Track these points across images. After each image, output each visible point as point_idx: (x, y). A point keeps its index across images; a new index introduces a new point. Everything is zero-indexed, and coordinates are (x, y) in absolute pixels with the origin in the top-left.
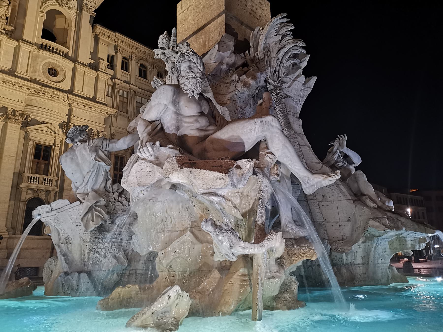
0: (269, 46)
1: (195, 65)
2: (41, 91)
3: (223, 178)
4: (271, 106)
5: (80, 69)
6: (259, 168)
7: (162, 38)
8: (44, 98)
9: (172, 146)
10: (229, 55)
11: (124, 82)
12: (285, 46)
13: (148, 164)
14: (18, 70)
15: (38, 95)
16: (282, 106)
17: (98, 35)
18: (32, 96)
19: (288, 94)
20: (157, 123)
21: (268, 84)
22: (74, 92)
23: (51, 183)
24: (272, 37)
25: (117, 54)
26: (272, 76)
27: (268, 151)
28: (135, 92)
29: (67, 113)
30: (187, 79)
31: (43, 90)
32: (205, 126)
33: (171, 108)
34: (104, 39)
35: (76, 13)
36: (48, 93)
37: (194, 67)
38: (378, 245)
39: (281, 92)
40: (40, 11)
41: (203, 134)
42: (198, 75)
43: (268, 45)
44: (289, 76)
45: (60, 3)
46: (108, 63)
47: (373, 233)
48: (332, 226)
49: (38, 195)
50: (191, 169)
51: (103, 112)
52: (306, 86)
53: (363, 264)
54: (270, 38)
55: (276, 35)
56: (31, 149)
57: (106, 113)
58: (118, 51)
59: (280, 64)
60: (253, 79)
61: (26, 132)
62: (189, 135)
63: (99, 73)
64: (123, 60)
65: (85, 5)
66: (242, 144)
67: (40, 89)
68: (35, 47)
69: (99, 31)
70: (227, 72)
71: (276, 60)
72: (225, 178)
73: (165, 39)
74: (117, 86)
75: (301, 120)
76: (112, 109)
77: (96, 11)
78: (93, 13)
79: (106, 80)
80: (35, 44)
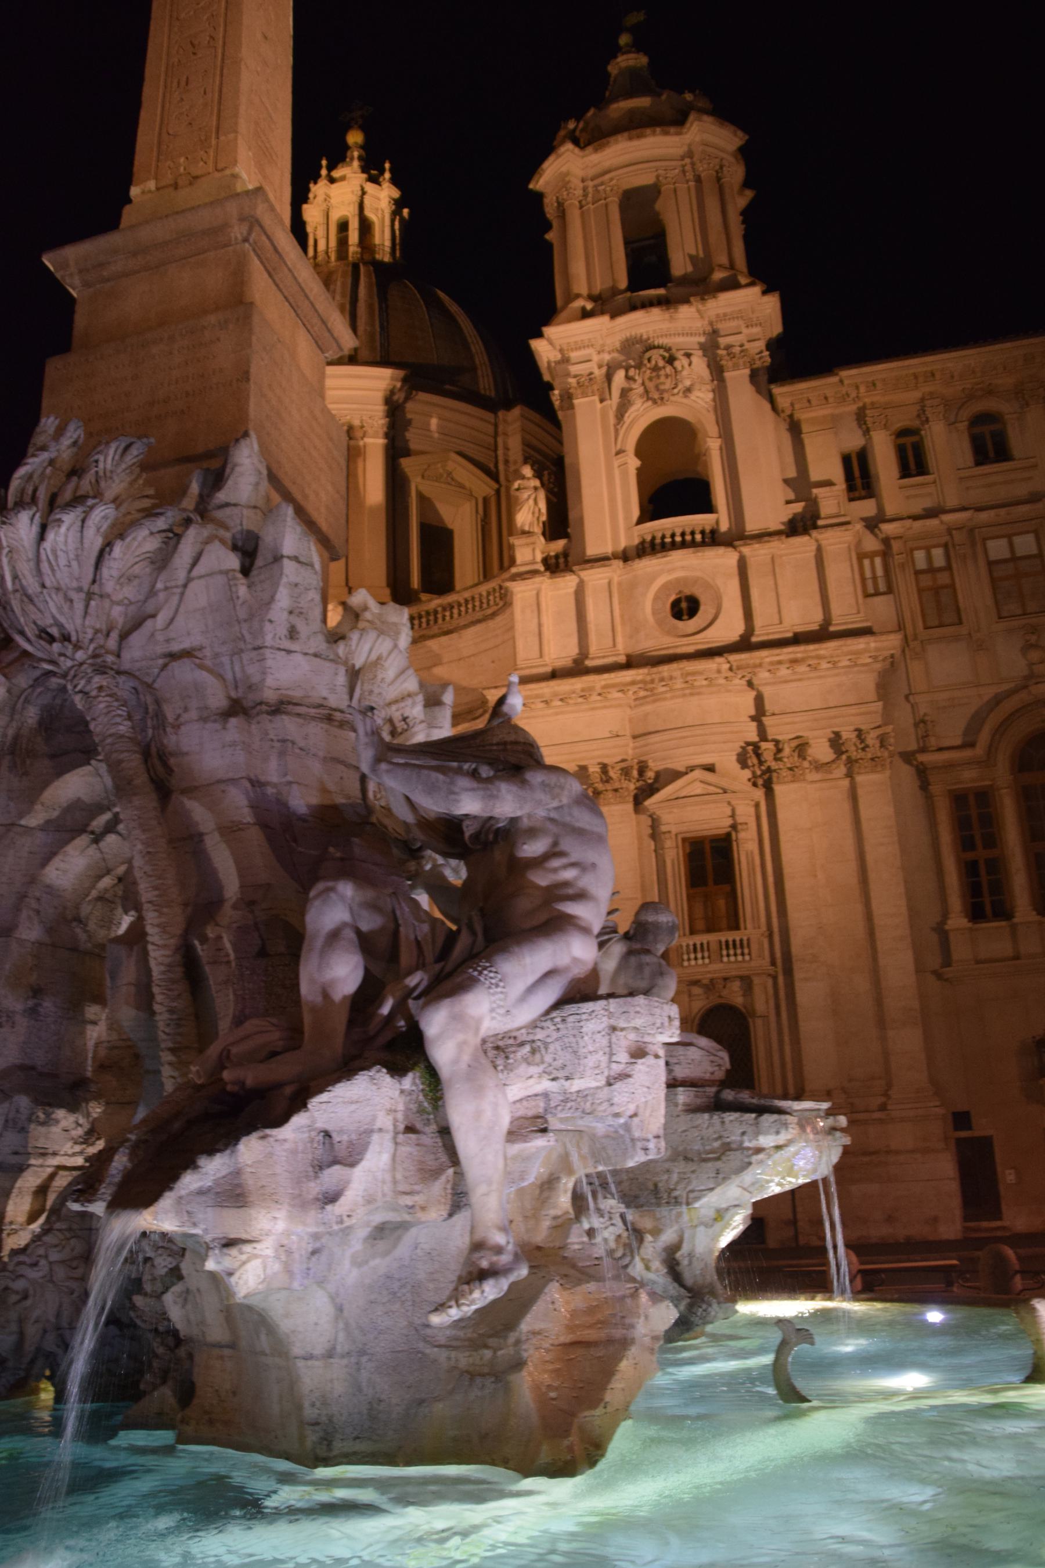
2: (652, 681)
8: (672, 698)
14: (593, 649)
15: (653, 695)
18: (641, 705)
19: (176, 647)
23: (746, 951)
25: (870, 438)
29: (753, 712)
31: (656, 677)
35: (713, 391)
36: (671, 678)
40: (618, 453)
45: (656, 396)
49: (720, 997)
51: (860, 662)
52: (259, 562)
56: (673, 861)
57: (870, 660)
61: (651, 816)
63: (820, 537)
67: (648, 678)
68: (618, 564)
69: (789, 400)
74: (896, 546)
78: (760, 358)
80: (615, 556)
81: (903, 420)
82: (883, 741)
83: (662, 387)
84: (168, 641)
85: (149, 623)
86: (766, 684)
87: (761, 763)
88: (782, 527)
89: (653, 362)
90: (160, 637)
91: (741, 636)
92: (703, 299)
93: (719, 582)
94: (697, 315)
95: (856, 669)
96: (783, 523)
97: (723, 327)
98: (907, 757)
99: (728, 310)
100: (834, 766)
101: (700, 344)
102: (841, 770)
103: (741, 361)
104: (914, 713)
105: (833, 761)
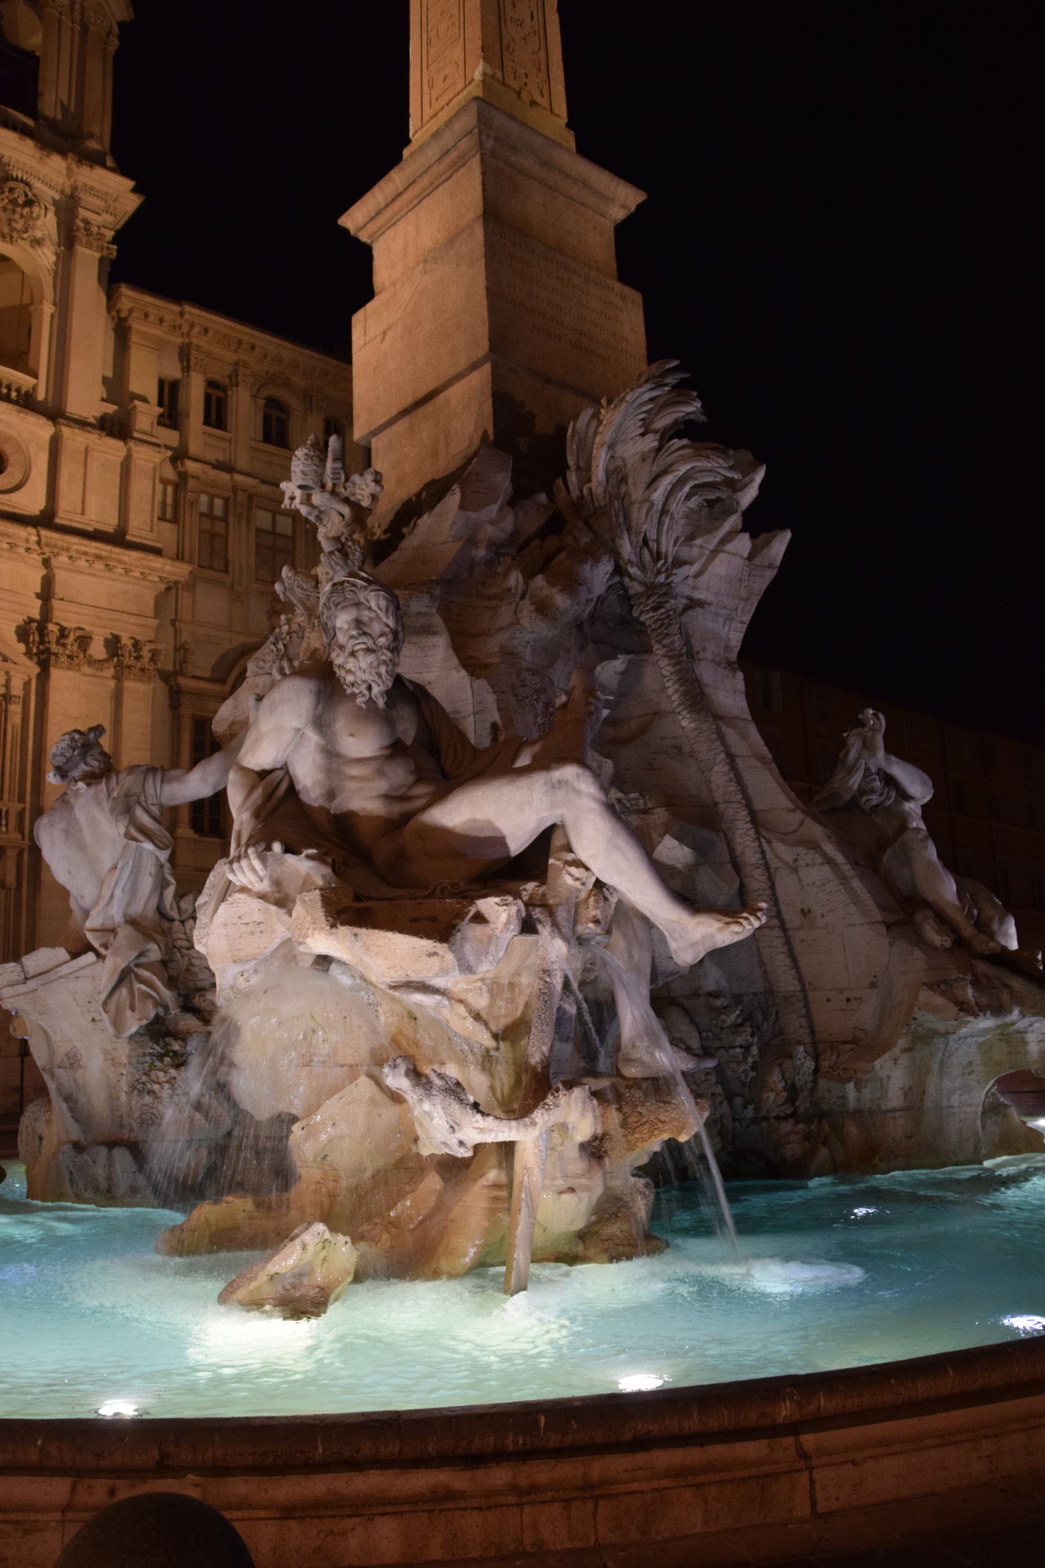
0: (625, 466)
1: (373, 615)
3: (435, 954)
4: (591, 713)
5: (74, 439)
6: (545, 906)
7: (302, 458)
9: (314, 851)
10: (494, 515)
11: (215, 467)
12: (671, 465)
13: (256, 904)
16: (672, 643)
17: (126, 319)
19: (697, 595)
20: (279, 774)
21: (627, 580)
22: (57, 521)
24: (632, 439)
25: (188, 376)
26: (635, 554)
27: (570, 857)
28: (251, 497)
29: (39, 590)
30: (353, 654)
32: (401, 786)
33: (313, 738)
34: (145, 329)
35: (57, 254)
37: (371, 619)
38: (952, 1054)
39: (666, 602)
41: (398, 808)
42: (382, 641)
43: (620, 463)
44: (698, 542)
46: (161, 410)
47: (933, 1026)
48: (828, 1000)
50: (357, 930)
51: (150, 578)
52: (757, 561)
53: (907, 1109)
54: (624, 441)
55: (643, 435)
57: (157, 579)
58: (192, 365)
59: (661, 515)
60: (562, 591)
62: (362, 814)
64: (211, 391)
65: (82, 225)
66: (500, 841)
69: (130, 305)
70: (490, 563)
71: (644, 510)
72: (440, 953)
73: (309, 462)
74: (191, 484)
75: (740, 675)
76: (178, 564)
77: (115, 240)
78: (108, 248)
79: (155, 468)
81: (219, 374)
82: (155, 655)
83: (14, 225)
84: (694, 588)
85: (687, 567)
86: (62, 568)
87: (42, 642)
88: (94, 422)
89: (16, 195)
90: (690, 581)
91: (41, 511)
92: (80, 162)
93: (32, 450)
94: (64, 172)
95: (144, 583)
96: (95, 418)
97: (86, 198)
98: (166, 677)
99: (97, 186)
100: (106, 665)
101: (53, 199)
102: (110, 672)
103: (95, 243)
104: (176, 639)
105: (105, 660)
